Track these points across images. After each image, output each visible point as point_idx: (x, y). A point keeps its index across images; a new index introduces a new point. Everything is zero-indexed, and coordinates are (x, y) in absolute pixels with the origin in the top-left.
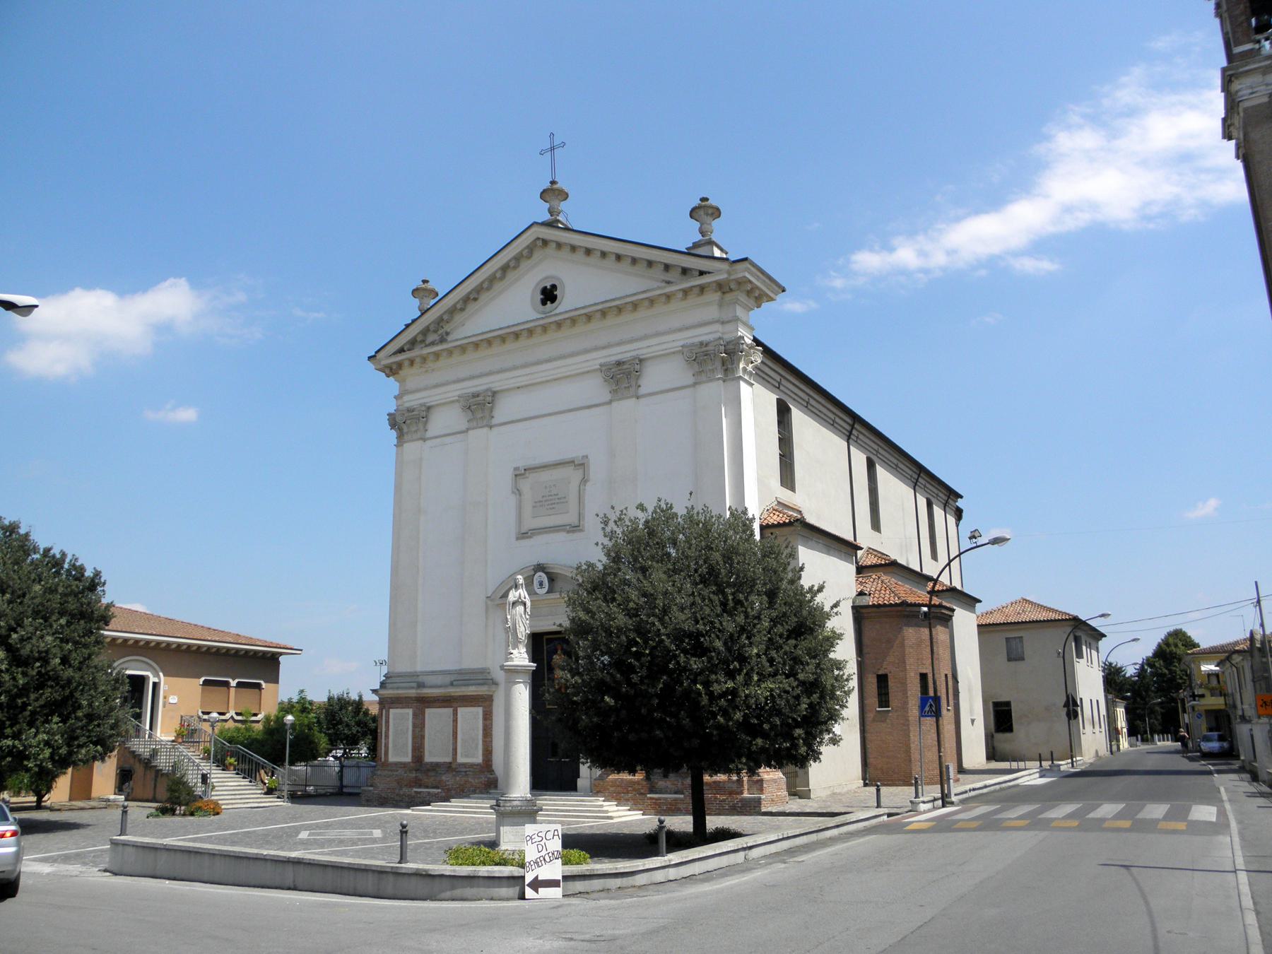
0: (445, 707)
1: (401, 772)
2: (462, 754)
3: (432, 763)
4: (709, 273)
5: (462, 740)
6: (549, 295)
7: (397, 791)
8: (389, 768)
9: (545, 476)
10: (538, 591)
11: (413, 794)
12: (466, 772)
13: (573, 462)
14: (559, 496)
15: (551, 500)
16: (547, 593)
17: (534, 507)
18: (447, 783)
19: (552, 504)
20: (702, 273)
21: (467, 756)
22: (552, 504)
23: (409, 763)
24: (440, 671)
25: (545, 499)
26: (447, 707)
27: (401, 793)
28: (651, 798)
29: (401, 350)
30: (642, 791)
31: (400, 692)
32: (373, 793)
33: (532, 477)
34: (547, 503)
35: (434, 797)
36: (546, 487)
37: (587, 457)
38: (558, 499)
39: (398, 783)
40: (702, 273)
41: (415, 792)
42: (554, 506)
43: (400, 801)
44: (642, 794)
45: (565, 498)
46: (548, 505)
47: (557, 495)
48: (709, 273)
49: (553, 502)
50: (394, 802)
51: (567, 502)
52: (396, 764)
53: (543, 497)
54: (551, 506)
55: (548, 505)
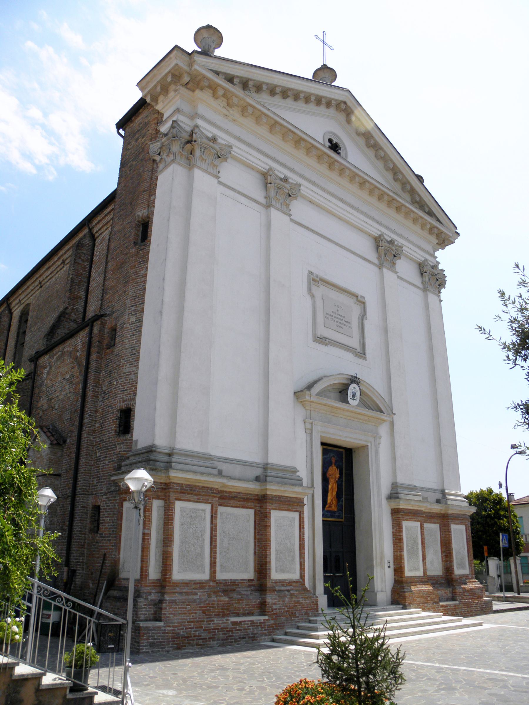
0: (243, 507)
1: (200, 595)
4: (441, 223)
5: (276, 550)
7: (205, 625)
8: (178, 590)
9: (334, 295)
10: (350, 401)
11: (230, 626)
13: (357, 297)
15: (339, 319)
16: (357, 405)
18: (274, 607)
21: (283, 571)
22: (340, 323)
24: (237, 460)
25: (334, 315)
26: (247, 508)
27: (212, 626)
28: (442, 606)
30: (436, 600)
31: (198, 477)
32: (164, 632)
34: (337, 320)
41: (234, 623)
43: (210, 638)
44: (436, 603)
47: (344, 317)
48: (441, 223)
49: (340, 321)
50: (200, 642)
52: (187, 583)
53: (333, 312)
54: (338, 324)
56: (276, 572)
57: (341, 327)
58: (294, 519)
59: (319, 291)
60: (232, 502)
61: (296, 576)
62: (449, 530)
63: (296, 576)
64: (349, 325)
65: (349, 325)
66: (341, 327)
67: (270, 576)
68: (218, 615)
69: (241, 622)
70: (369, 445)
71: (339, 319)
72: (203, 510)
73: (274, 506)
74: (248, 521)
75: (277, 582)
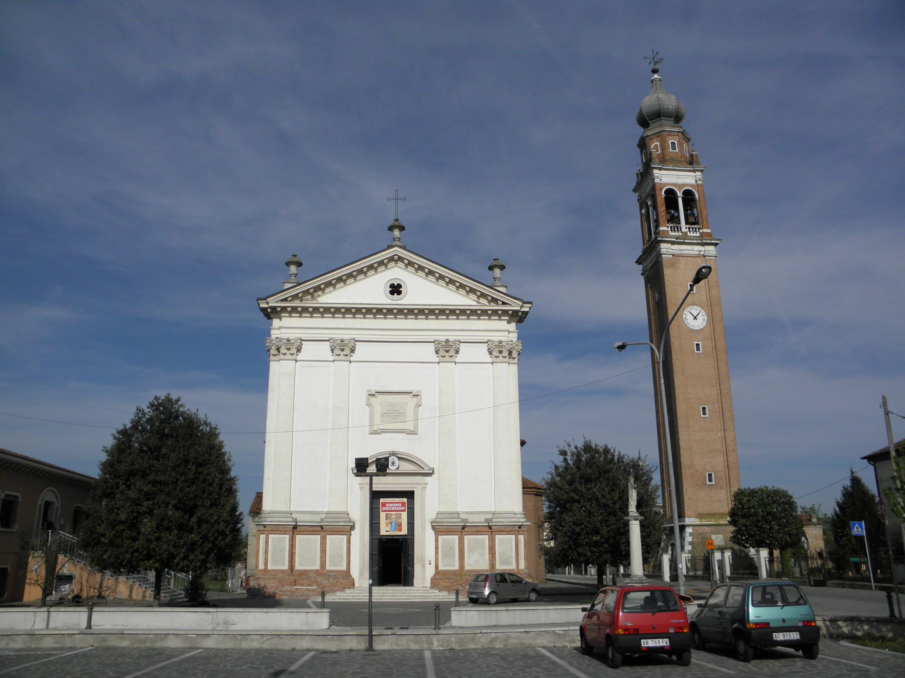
2: (330, 564)
3: (301, 570)
6: (396, 289)
7: (280, 589)
8: (270, 573)
9: (390, 398)
11: (294, 590)
12: (335, 575)
13: (412, 393)
14: (400, 412)
15: (395, 413)
17: (381, 416)
18: (322, 583)
19: (395, 416)
20: (504, 303)
22: (395, 416)
23: (286, 570)
24: (309, 512)
25: (389, 412)
27: (284, 589)
29: (285, 300)
33: (380, 396)
35: (312, 592)
36: (390, 405)
37: (420, 391)
38: (399, 413)
39: (280, 583)
40: (504, 303)
41: (295, 589)
42: (396, 417)
45: (404, 413)
46: (392, 416)
47: (399, 411)
51: (405, 416)
53: (388, 411)
55: (392, 416)
56: (330, 566)
57: (396, 418)
58: (343, 539)
59: (376, 401)
60: (305, 533)
61: (344, 568)
62: (494, 539)
63: (344, 568)
64: (404, 415)
65: (404, 415)
66: (396, 418)
67: (295, 568)
68: (288, 584)
69: (300, 589)
70: (415, 490)
71: (395, 413)
72: (299, 539)
73: (328, 533)
74: (316, 541)
75: (329, 571)
